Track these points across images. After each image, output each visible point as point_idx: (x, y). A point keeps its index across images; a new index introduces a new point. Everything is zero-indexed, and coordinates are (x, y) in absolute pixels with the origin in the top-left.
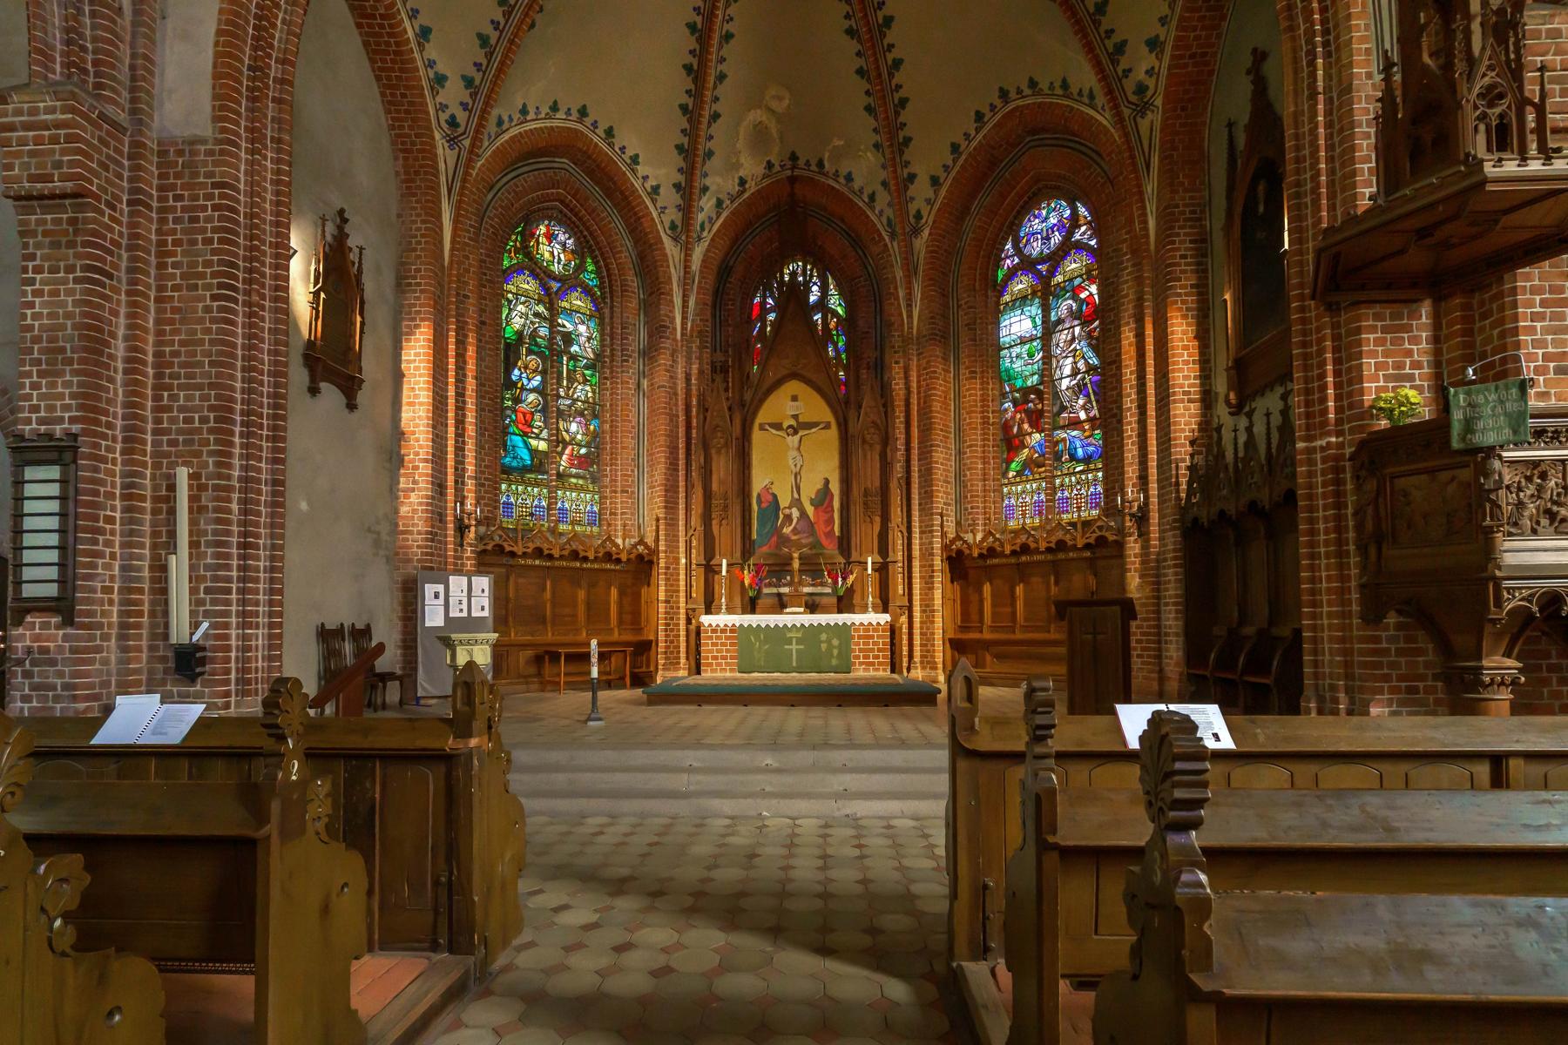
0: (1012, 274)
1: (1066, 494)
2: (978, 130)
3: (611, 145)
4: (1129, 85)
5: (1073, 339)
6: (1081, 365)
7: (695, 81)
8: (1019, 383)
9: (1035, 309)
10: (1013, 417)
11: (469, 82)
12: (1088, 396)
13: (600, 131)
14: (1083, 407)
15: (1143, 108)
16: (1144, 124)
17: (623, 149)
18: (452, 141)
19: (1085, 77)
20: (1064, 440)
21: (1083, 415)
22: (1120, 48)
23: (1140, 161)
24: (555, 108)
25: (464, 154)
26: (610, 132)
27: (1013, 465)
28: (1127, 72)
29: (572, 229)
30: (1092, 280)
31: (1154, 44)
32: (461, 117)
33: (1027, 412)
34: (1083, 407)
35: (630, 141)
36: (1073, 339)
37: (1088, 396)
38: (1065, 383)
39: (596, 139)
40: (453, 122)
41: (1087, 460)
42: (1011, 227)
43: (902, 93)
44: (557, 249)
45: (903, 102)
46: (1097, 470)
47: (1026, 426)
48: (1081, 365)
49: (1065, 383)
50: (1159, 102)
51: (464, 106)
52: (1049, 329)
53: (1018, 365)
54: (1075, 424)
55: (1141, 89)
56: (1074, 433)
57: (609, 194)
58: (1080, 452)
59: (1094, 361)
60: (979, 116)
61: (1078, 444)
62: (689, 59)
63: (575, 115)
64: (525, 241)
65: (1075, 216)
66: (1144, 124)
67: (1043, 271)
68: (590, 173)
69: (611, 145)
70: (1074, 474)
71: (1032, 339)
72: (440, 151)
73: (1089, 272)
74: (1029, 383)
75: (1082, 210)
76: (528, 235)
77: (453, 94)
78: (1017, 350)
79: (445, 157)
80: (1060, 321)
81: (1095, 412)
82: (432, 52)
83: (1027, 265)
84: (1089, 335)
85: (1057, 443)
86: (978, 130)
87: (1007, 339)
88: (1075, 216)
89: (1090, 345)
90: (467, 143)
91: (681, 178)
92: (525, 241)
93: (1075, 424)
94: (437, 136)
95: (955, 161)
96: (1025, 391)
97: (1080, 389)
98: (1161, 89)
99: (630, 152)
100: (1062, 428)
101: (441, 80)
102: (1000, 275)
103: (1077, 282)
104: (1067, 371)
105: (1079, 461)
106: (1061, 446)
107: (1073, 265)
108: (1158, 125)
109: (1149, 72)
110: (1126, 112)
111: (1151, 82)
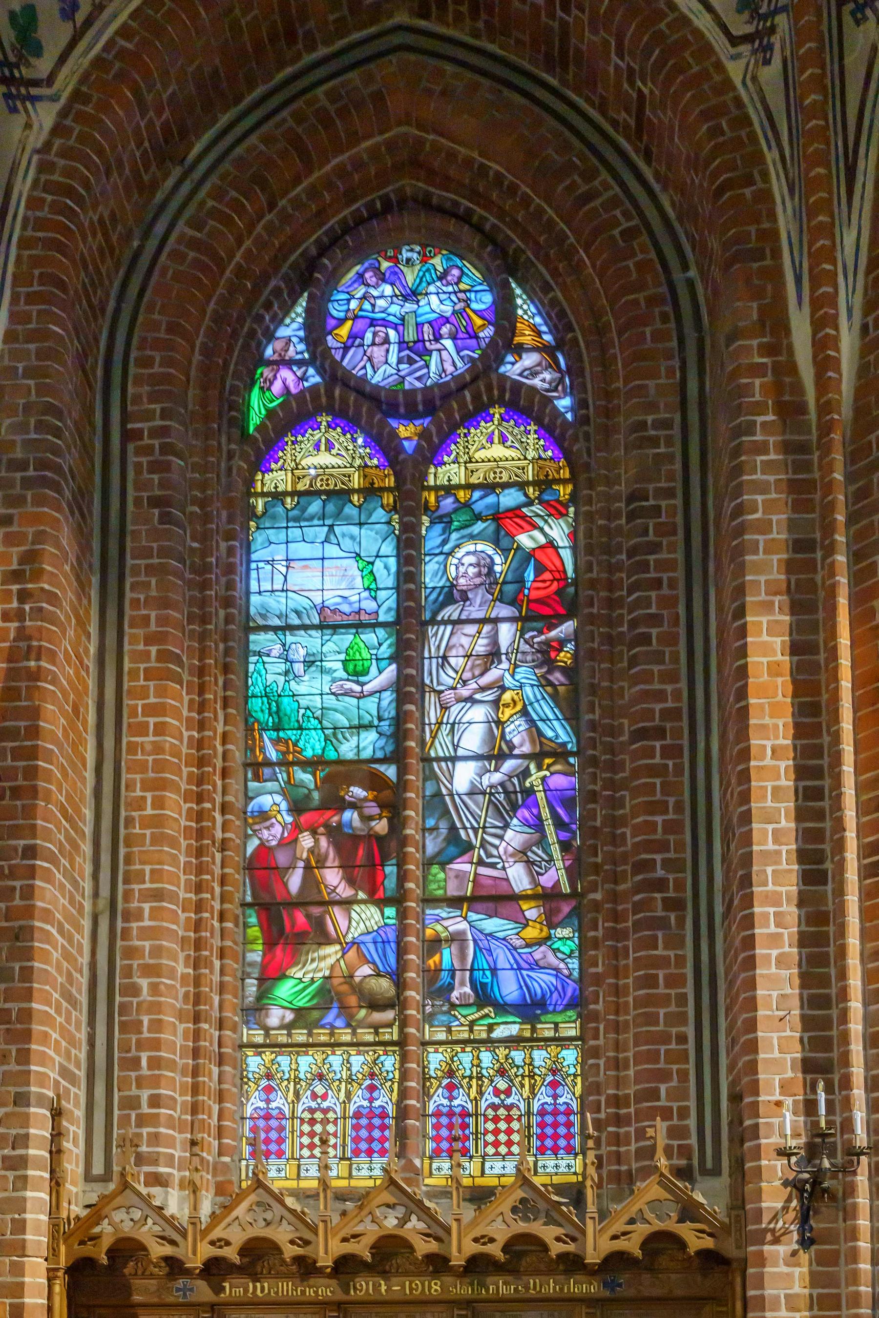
0: (294, 417)
1: (461, 1100)
5: (493, 655)
8: (312, 744)
9: (376, 539)
10: (290, 842)
12: (538, 825)
14: (522, 855)
20: (457, 938)
21: (518, 878)
27: (285, 990)
30: (556, 510)
34: (522, 855)
36: (493, 655)
37: (538, 825)
41: (530, 1009)
46: (562, 1042)
47: (332, 877)
48: (517, 732)
53: (310, 688)
56: (492, 925)
59: (558, 731)
61: (503, 958)
67: (405, 432)
70: (490, 1043)
73: (544, 484)
74: (347, 750)
78: (304, 644)
80: (452, 594)
81: (556, 875)
83: (346, 401)
84: (546, 656)
87: (277, 604)
89: (544, 682)
93: (496, 899)
96: (338, 774)
97: (513, 800)
102: (258, 407)
103: (510, 499)
104: (473, 740)
105: (502, 1008)
106: (447, 957)
107: (495, 451)
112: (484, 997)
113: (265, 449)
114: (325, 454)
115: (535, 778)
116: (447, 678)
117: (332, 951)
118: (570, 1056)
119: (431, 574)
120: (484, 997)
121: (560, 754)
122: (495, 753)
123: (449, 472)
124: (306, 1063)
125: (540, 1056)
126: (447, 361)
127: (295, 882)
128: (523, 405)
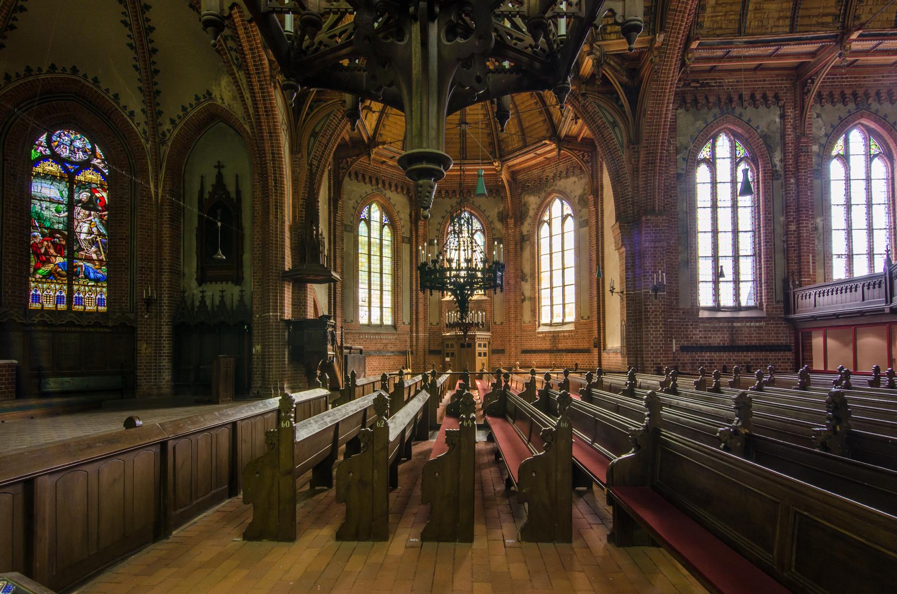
0: (44, 158)
1: (81, 295)
2: (48, 72)
6: (95, 230)
8: (48, 224)
14: (95, 252)
15: (163, 143)
16: (163, 149)
21: (94, 256)
28: (161, 124)
31: (173, 122)
33: (53, 243)
34: (95, 252)
38: (83, 236)
41: (97, 280)
43: (15, 23)
45: (12, 27)
47: (52, 251)
48: (95, 230)
49: (83, 236)
50: (170, 144)
52: (71, 204)
53: (46, 213)
54: (89, 260)
55: (164, 134)
58: (92, 275)
59: (103, 231)
61: (91, 271)
66: (163, 149)
70: (88, 286)
71: (59, 203)
74: (56, 227)
75: (98, 151)
78: (45, 204)
81: (103, 257)
84: (101, 217)
85: (76, 266)
86: (48, 72)
88: (93, 150)
89: (101, 222)
93: (89, 260)
96: (53, 232)
97: (93, 243)
100: (81, 259)
102: (34, 155)
103: (94, 186)
104: (85, 230)
105: (91, 280)
107: (88, 176)
108: (167, 152)
109: (169, 130)
110: (157, 140)
111: (168, 135)
112: (87, 277)
113: (37, 162)
114: (52, 167)
115: (98, 239)
116: (79, 217)
117: (52, 265)
118: (105, 290)
119: (76, 196)
120: (87, 277)
121: (104, 235)
122: (90, 233)
123: (80, 178)
124: (45, 286)
125: (98, 289)
126: (80, 156)
127: (43, 250)
128: (97, 169)
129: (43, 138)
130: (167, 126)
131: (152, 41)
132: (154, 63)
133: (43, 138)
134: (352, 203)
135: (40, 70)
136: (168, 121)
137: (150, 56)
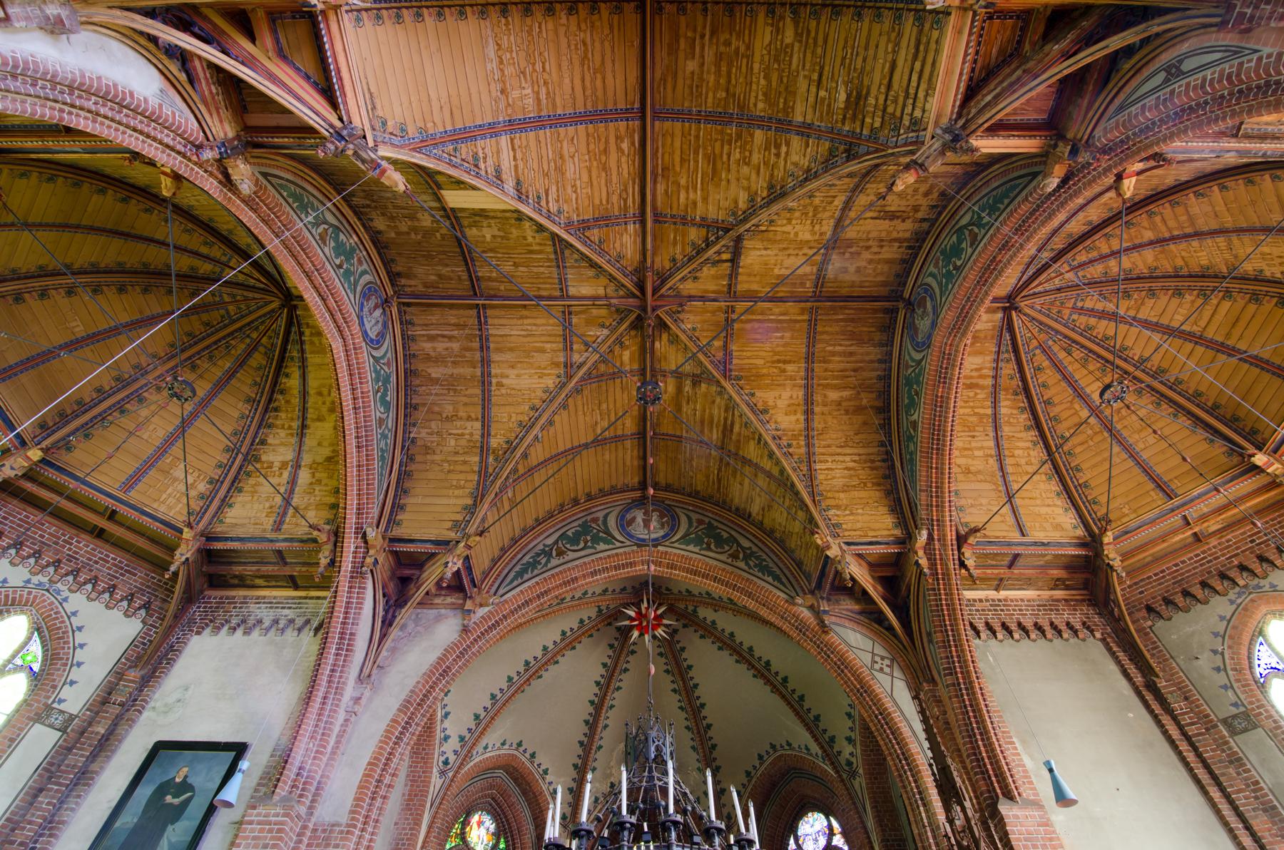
2: (761, 764)
3: (532, 763)
4: (842, 760)
7: (590, 729)
11: (462, 739)
13: (527, 755)
15: (853, 774)
16: (856, 783)
17: (539, 765)
18: (442, 773)
19: (815, 748)
22: (832, 739)
23: (860, 806)
24: (503, 744)
25: (448, 781)
26: (533, 755)
28: (839, 753)
29: (496, 818)
32: (452, 758)
35: (544, 760)
39: (524, 759)
40: (446, 762)
42: (792, 829)
43: (713, 742)
44: (483, 831)
45: (714, 747)
50: (861, 771)
51: (455, 752)
55: (849, 763)
57: (524, 793)
60: (760, 757)
62: (588, 717)
63: (515, 746)
64: (463, 829)
65: (830, 827)
66: (856, 783)
68: (515, 780)
69: (532, 763)
72: (433, 780)
76: (466, 823)
77: (453, 743)
79: (436, 782)
82: (447, 724)
86: (761, 764)
88: (830, 827)
90: (451, 774)
91: (574, 785)
92: (463, 829)
94: (435, 770)
95: (749, 781)
98: (860, 760)
99: (543, 767)
101: (446, 738)
108: (864, 785)
109: (851, 754)
110: (845, 776)
111: (854, 760)
129: (792, 841)
130: (848, 749)
131: (777, 673)
132: (794, 691)
133: (792, 841)
134: (1205, 663)
135: (755, 767)
136: (845, 743)
137: (786, 687)
